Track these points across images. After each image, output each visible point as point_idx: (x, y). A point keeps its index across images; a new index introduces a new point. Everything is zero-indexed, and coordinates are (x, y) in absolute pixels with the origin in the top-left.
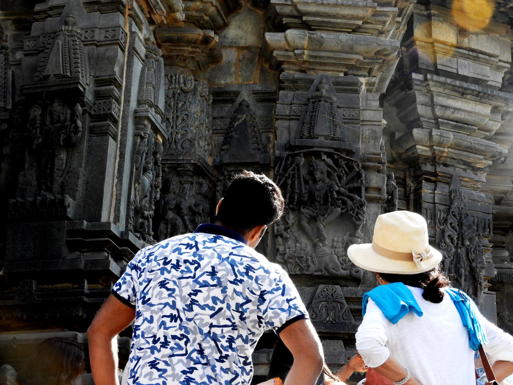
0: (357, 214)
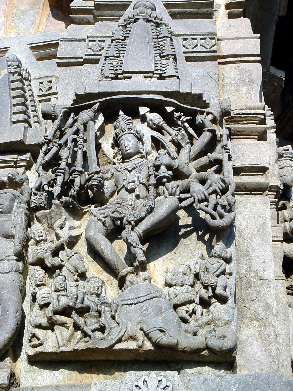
0: (215, 209)
